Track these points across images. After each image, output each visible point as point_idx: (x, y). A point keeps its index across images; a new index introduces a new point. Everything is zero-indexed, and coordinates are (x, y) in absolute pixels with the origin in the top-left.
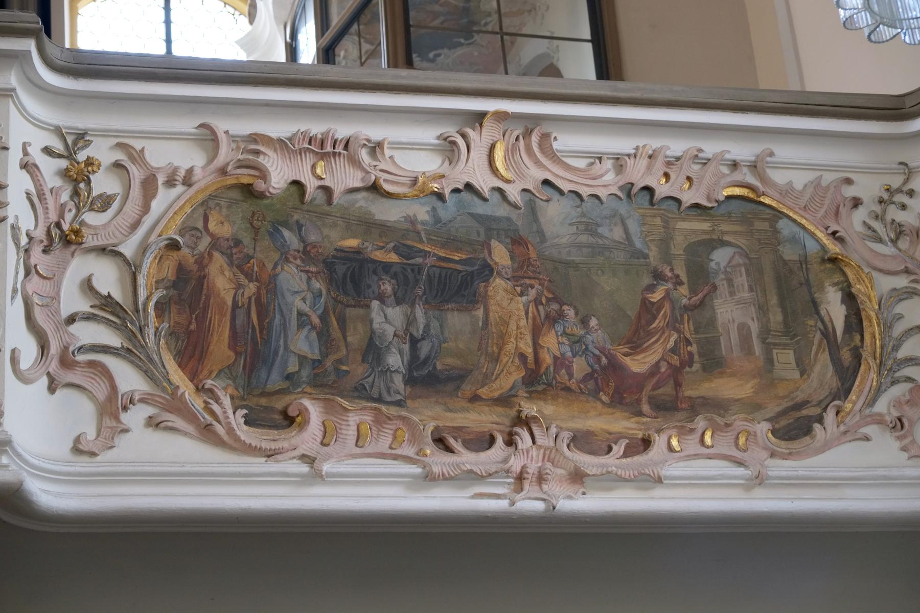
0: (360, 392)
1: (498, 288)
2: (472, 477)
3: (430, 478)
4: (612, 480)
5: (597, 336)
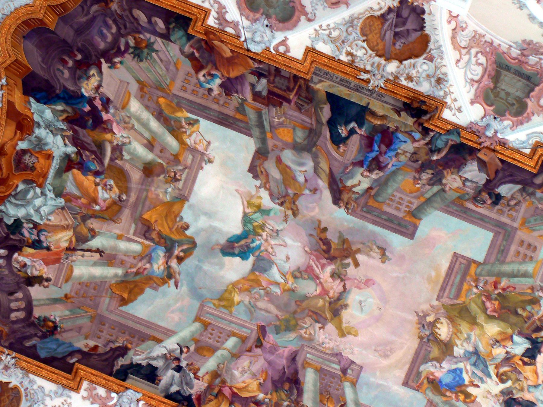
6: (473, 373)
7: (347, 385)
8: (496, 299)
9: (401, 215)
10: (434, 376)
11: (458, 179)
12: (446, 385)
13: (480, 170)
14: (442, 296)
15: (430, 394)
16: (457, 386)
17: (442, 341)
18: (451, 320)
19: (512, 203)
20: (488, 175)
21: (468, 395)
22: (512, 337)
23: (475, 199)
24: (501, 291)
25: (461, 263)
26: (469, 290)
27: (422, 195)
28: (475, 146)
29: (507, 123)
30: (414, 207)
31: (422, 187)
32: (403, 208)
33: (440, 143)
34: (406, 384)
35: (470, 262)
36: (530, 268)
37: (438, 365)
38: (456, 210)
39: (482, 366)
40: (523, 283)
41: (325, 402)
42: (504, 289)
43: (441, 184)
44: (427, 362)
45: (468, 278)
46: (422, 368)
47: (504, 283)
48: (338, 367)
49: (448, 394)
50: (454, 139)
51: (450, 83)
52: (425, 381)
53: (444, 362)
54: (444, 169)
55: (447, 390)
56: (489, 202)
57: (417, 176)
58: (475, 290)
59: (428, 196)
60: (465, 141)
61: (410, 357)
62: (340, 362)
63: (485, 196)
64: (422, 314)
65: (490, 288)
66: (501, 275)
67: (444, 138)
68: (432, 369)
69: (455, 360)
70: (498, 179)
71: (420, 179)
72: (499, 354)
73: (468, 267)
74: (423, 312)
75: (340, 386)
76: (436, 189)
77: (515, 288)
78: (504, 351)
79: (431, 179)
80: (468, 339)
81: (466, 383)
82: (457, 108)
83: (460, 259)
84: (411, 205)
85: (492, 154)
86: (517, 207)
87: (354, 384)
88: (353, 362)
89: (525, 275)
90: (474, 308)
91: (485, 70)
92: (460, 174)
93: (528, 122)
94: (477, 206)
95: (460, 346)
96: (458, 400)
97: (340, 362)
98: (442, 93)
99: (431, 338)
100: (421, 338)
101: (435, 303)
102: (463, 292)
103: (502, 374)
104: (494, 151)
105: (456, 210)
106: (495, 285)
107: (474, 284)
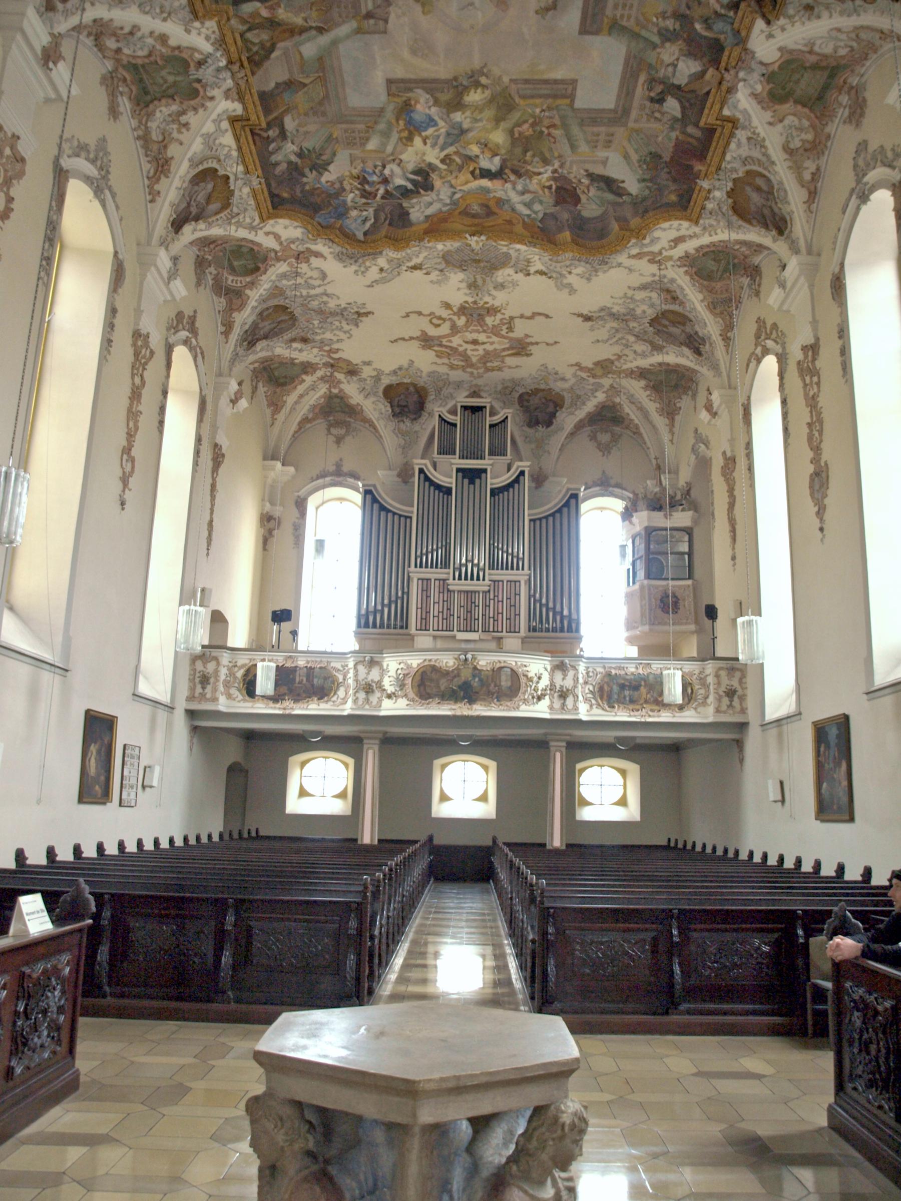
0: (623, 703)
1: (642, 688)
2: (635, 716)
3: (630, 716)
4: (654, 716)
5: (655, 695)
6: (438, 137)
7: (354, 24)
8: (534, 131)
9: (609, 12)
10: (415, 104)
11: (676, 57)
12: (411, 117)
13: (690, 76)
14: (517, 84)
15: (391, 107)
16: (415, 127)
17: (461, 98)
18: (492, 100)
19: (657, 115)
20: (686, 85)
21: (410, 139)
22: (497, 155)
23: (652, 81)
24: (546, 132)
25: (566, 90)
26: (536, 106)
27: (644, 27)
28: (723, 64)
29: (759, 88)
30: (624, 23)
31: (653, 23)
32: (618, 13)
33: (719, 26)
34: (390, 82)
35: (572, 97)
36: (584, 148)
37: (431, 103)
38: (632, 67)
39: (450, 141)
40: (563, 147)
41: (314, 9)
42: (549, 134)
43: (663, 43)
44: (428, 93)
45: (550, 101)
46: (419, 91)
47: (557, 133)
48: (370, 6)
49: (401, 123)
50: (728, 40)
51: (807, 23)
52: (404, 99)
53: (437, 108)
54: (685, 40)
55: (405, 120)
56: (652, 94)
57: (668, 14)
58: (538, 111)
59: (644, 33)
60: (726, 53)
61: (425, 75)
62: (379, 7)
63: (659, 88)
64: (485, 71)
65: (546, 122)
66: (565, 126)
67: (728, 28)
68: (422, 100)
69: (445, 117)
70: (684, 94)
71: (664, 18)
72: (471, 150)
73: (564, 97)
74: (489, 71)
75: (347, 17)
76: (656, 39)
77: (554, 143)
78: (478, 153)
79: (667, 30)
80: (476, 120)
81: (424, 134)
82: (773, 33)
83: (571, 87)
84: (625, 19)
85: (715, 83)
86: (653, 120)
87: (359, 31)
88: (386, 21)
89: (573, 147)
90: (516, 116)
91: (825, 56)
92: (682, 58)
93: (763, 108)
94: (643, 85)
95: (463, 116)
96: (400, 132)
97: (379, 7)
98: (791, 12)
99: (460, 88)
100: (455, 79)
101: (506, 79)
102: (531, 101)
103: (450, 159)
104: (720, 83)
105: (632, 67)
106: (554, 126)
107: (544, 107)
